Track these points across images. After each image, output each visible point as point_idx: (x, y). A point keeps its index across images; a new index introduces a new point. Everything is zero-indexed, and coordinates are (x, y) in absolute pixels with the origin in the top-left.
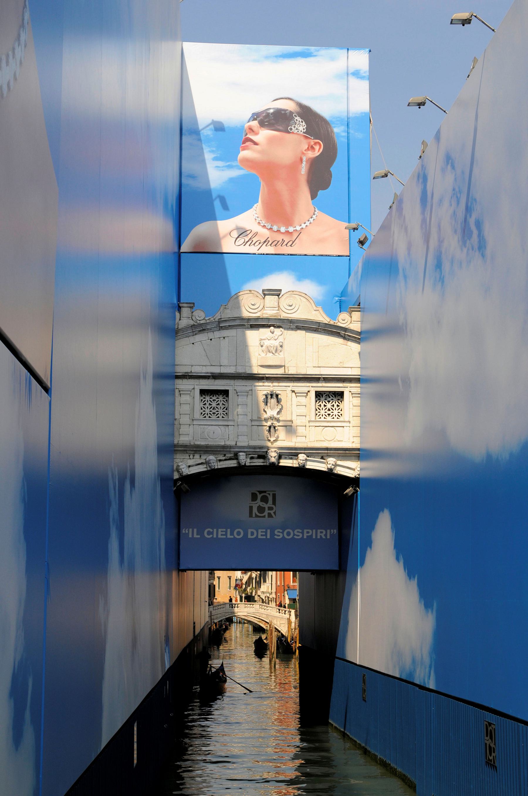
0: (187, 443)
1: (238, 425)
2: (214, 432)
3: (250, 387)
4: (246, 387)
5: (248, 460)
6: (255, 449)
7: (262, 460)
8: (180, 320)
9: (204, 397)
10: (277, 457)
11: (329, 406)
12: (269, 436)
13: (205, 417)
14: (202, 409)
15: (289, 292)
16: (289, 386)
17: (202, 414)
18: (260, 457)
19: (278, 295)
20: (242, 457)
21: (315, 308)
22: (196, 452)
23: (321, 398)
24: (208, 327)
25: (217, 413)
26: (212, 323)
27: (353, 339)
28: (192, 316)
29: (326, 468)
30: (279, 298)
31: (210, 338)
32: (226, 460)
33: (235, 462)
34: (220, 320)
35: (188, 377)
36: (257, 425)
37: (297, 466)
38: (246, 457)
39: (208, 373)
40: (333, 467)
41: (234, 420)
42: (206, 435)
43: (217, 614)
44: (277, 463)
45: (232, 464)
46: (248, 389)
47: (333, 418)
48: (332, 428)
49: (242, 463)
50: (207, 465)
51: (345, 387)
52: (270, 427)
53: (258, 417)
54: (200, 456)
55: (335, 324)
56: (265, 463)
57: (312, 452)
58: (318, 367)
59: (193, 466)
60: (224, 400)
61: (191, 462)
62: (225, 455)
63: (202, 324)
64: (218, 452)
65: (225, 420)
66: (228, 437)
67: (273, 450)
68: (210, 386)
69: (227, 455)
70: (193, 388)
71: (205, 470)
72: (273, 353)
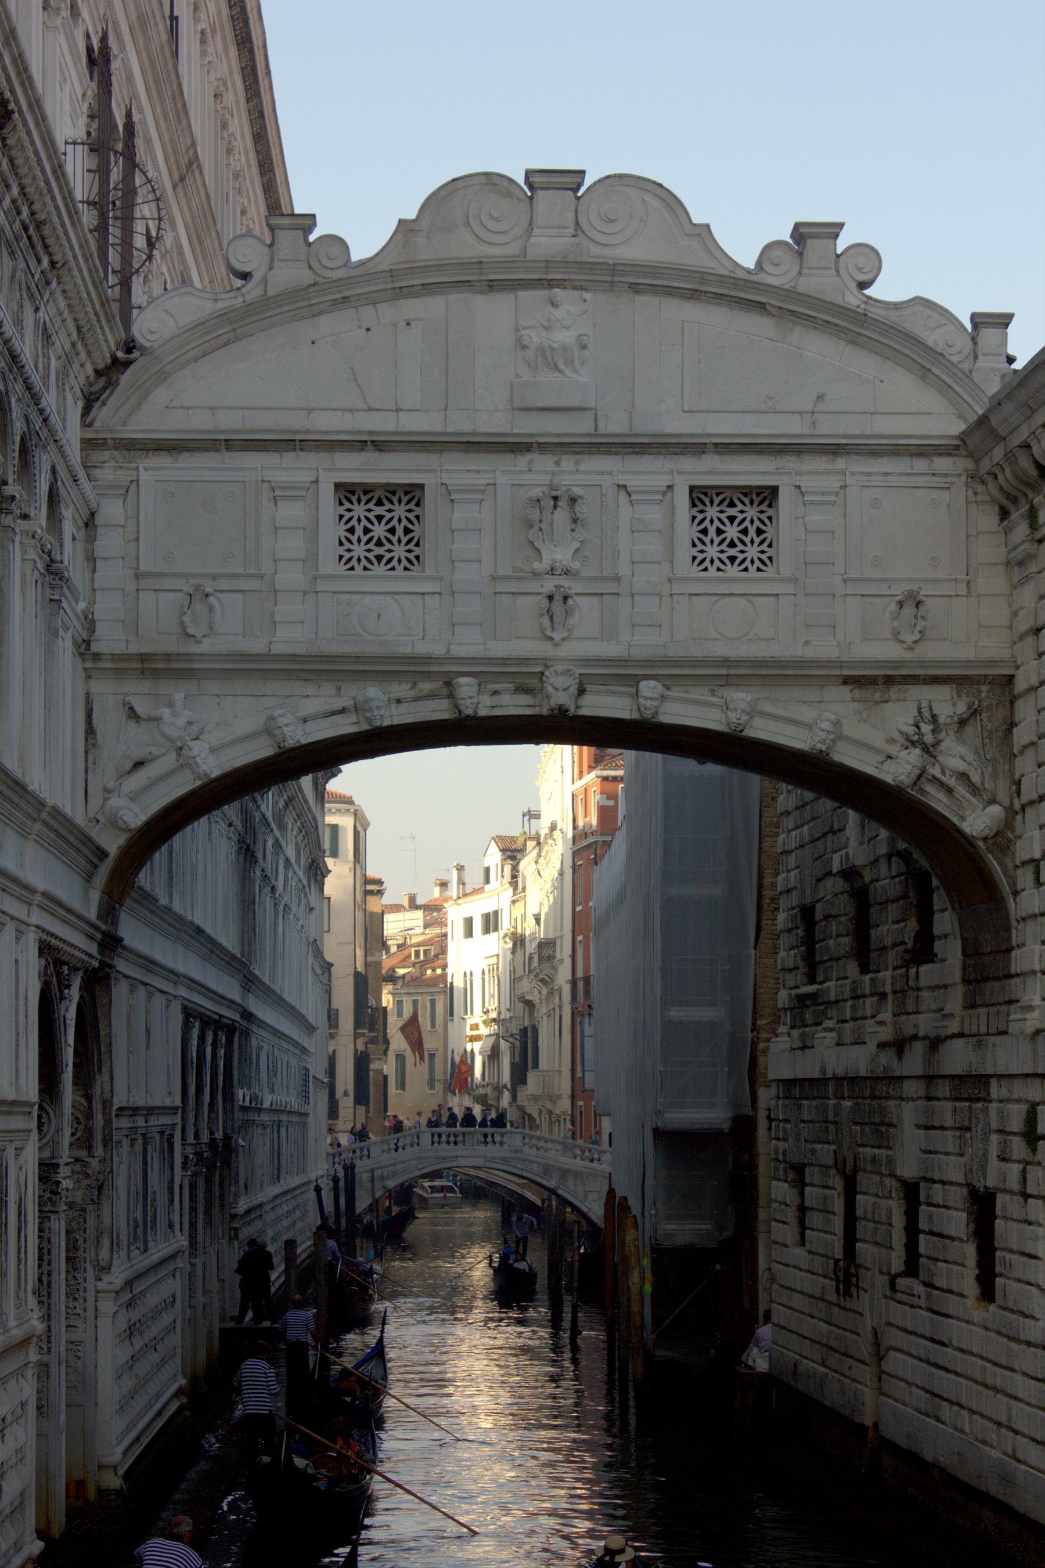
0: (300, 650)
1: (453, 593)
2: (379, 616)
7: (525, 699)
8: (271, 268)
9: (347, 505)
10: (572, 688)
11: (732, 532)
15: (608, 177)
16: (610, 473)
20: (466, 687)
23: (708, 509)
24: (359, 291)
25: (388, 556)
29: (724, 721)
31: (365, 325)
32: (417, 699)
33: (445, 703)
34: (394, 267)
35: (298, 447)
36: (513, 593)
37: (636, 716)
38: (479, 692)
40: (744, 718)
41: (441, 579)
45: (437, 710)
46: (481, 480)
47: (746, 569)
48: (742, 602)
49: (467, 707)
50: (358, 717)
51: (778, 472)
52: (551, 598)
53: (513, 568)
54: (339, 689)
56: (537, 708)
58: (699, 412)
59: (315, 717)
61: (312, 706)
63: (340, 280)
66: (424, 630)
70: (314, 479)
72: (560, 371)
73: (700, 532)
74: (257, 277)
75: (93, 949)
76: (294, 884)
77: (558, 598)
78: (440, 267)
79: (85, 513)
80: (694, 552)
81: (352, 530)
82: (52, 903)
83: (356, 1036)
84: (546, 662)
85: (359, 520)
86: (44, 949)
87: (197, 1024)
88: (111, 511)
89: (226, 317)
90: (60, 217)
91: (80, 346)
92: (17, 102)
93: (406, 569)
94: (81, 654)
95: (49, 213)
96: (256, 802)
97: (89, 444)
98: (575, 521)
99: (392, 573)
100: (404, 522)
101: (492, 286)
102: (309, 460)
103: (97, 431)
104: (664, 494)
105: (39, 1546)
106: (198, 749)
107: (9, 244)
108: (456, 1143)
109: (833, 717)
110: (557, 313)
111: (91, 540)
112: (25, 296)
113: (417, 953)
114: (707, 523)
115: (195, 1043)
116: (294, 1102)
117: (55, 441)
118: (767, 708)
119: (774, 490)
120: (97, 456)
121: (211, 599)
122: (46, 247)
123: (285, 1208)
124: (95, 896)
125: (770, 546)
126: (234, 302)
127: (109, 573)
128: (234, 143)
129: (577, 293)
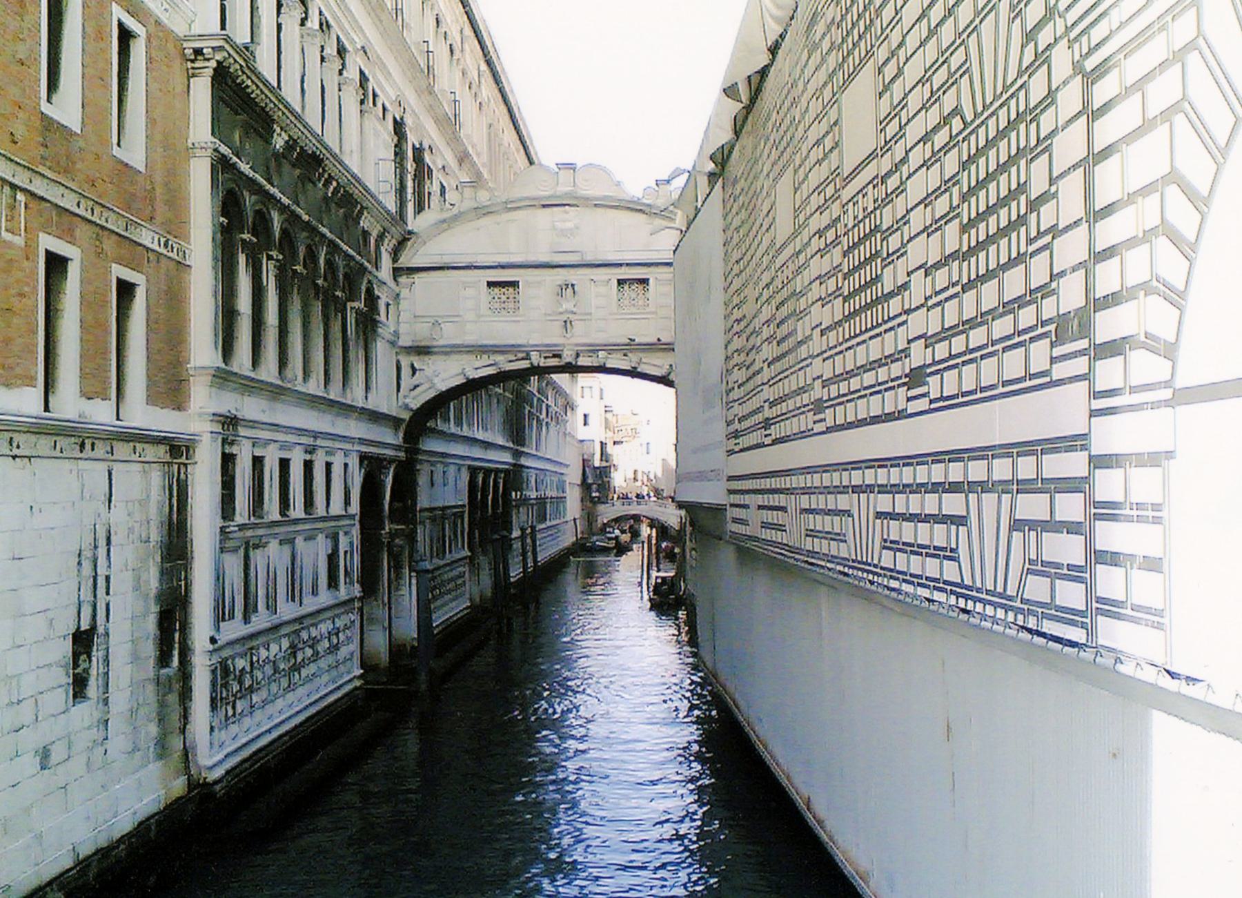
5: (543, 360)
7: (557, 359)
11: (633, 295)
18: (555, 356)
22: (484, 352)
26: (498, 204)
45: (524, 364)
46: (539, 279)
52: (565, 322)
57: (611, 348)
61: (478, 364)
75: (402, 455)
78: (520, 200)
82: (362, 441)
84: (564, 345)
86: (363, 457)
88: (404, 293)
89: (444, 221)
97: (395, 270)
101: (544, 206)
106: (436, 380)
111: (398, 304)
119: (648, 279)
121: (442, 325)
124: (401, 435)
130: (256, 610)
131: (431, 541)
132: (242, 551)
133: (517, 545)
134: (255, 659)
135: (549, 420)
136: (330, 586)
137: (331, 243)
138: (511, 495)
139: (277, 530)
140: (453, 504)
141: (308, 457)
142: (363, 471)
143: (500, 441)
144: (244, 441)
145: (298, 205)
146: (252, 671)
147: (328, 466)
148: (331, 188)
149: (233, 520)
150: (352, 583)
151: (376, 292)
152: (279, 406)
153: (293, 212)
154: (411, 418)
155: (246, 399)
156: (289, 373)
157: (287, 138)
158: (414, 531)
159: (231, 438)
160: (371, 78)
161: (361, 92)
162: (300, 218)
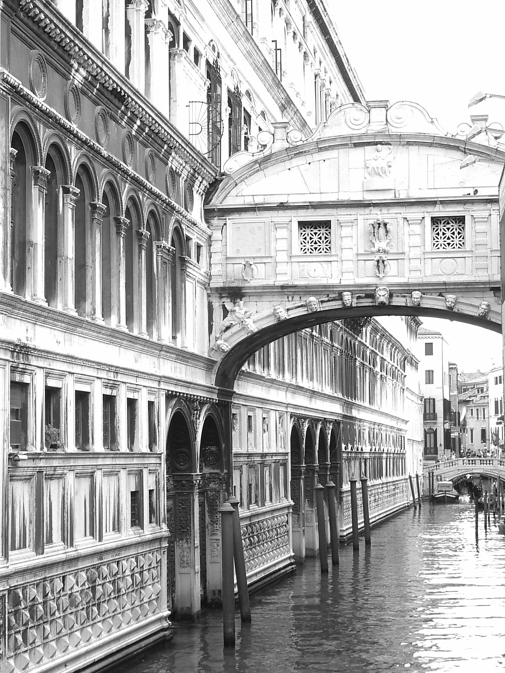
3: (356, 216)
4: (350, 216)
5: (355, 301)
6: (361, 287)
7: (370, 300)
8: (273, 143)
9: (304, 229)
10: (386, 295)
11: (448, 234)
12: (377, 271)
13: (306, 253)
14: (302, 244)
16: (401, 213)
17: (303, 250)
18: (368, 296)
19: (386, 107)
20: (347, 297)
21: (430, 120)
24: (305, 150)
25: (319, 247)
27: (475, 153)
28: (287, 137)
30: (387, 111)
31: (308, 162)
32: (329, 301)
33: (340, 302)
36: (365, 260)
37: (411, 305)
39: (306, 202)
40: (453, 305)
42: (306, 274)
43: (449, 472)
44: (387, 303)
45: (336, 305)
46: (352, 218)
52: (378, 261)
55: (454, 138)
60: (327, 232)
61: (289, 305)
62: (328, 296)
64: (320, 293)
65: (328, 255)
67: (381, 288)
68: (309, 218)
69: (330, 296)
71: (306, 313)
72: (381, 176)
73: (437, 234)
74: (268, 146)
75: (215, 397)
76: (390, 366)
77: (381, 261)
78: (334, 139)
79: (206, 237)
80: (434, 242)
81: (305, 239)
82: (168, 379)
83: (444, 423)
85: (308, 235)
86: (170, 396)
87: (307, 422)
88: (217, 235)
89: (256, 162)
90: (165, 131)
91: (196, 175)
92: (125, 92)
93: (326, 252)
94: (206, 288)
95: (159, 131)
96: (354, 337)
98: (387, 232)
99: (320, 254)
100: (325, 235)
101: (356, 145)
102: (289, 213)
103: (211, 206)
104: (421, 220)
105: (170, 612)
106: (249, 322)
107: (140, 142)
108: (490, 464)
109: (486, 303)
110: (378, 154)
111: (210, 246)
112: (157, 160)
113: (478, 392)
114: (439, 230)
115: (306, 429)
116: (392, 449)
117: (176, 212)
118: (462, 300)
120: (211, 215)
121: (253, 266)
122: (165, 142)
123: (385, 489)
124: (214, 377)
125: (463, 238)
126: (260, 156)
127: (215, 258)
128: (330, 92)
129: (387, 146)
130: (50, 540)
131: (250, 485)
132: (34, 480)
133: (347, 498)
134: (48, 589)
135: (384, 374)
136: (133, 524)
137: (135, 180)
138: (341, 447)
139: (72, 463)
140: (275, 451)
141: (108, 392)
142: (170, 410)
143: (328, 390)
144: (38, 371)
145: (98, 141)
146: (45, 603)
147: (132, 403)
148: (136, 127)
149: (26, 450)
150: (158, 523)
151: (185, 232)
152: (76, 339)
153: (92, 148)
154: (224, 360)
155: (37, 327)
156: (88, 308)
157: (84, 73)
158: (230, 475)
159: (21, 366)
160: (181, 21)
161: (170, 34)
162: (100, 154)
